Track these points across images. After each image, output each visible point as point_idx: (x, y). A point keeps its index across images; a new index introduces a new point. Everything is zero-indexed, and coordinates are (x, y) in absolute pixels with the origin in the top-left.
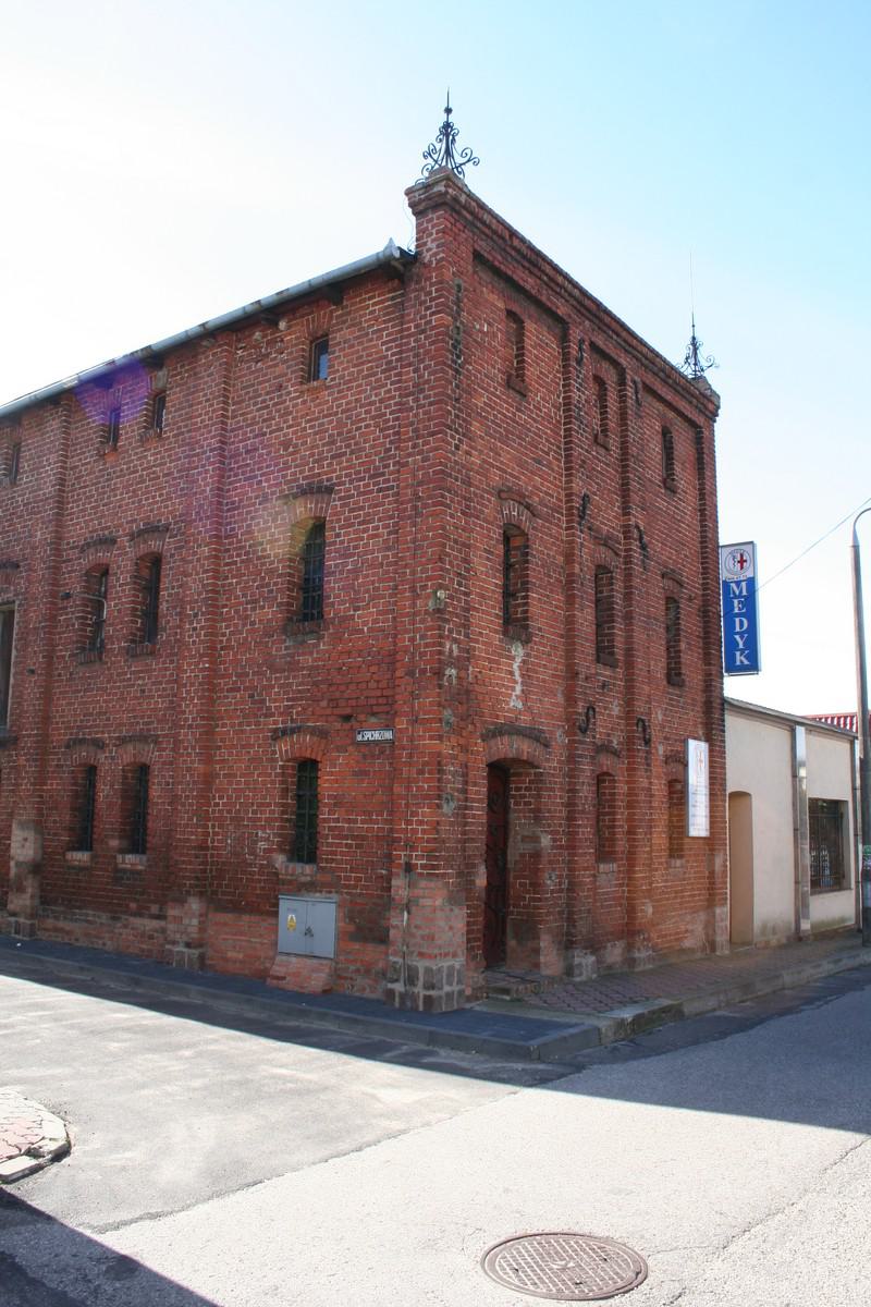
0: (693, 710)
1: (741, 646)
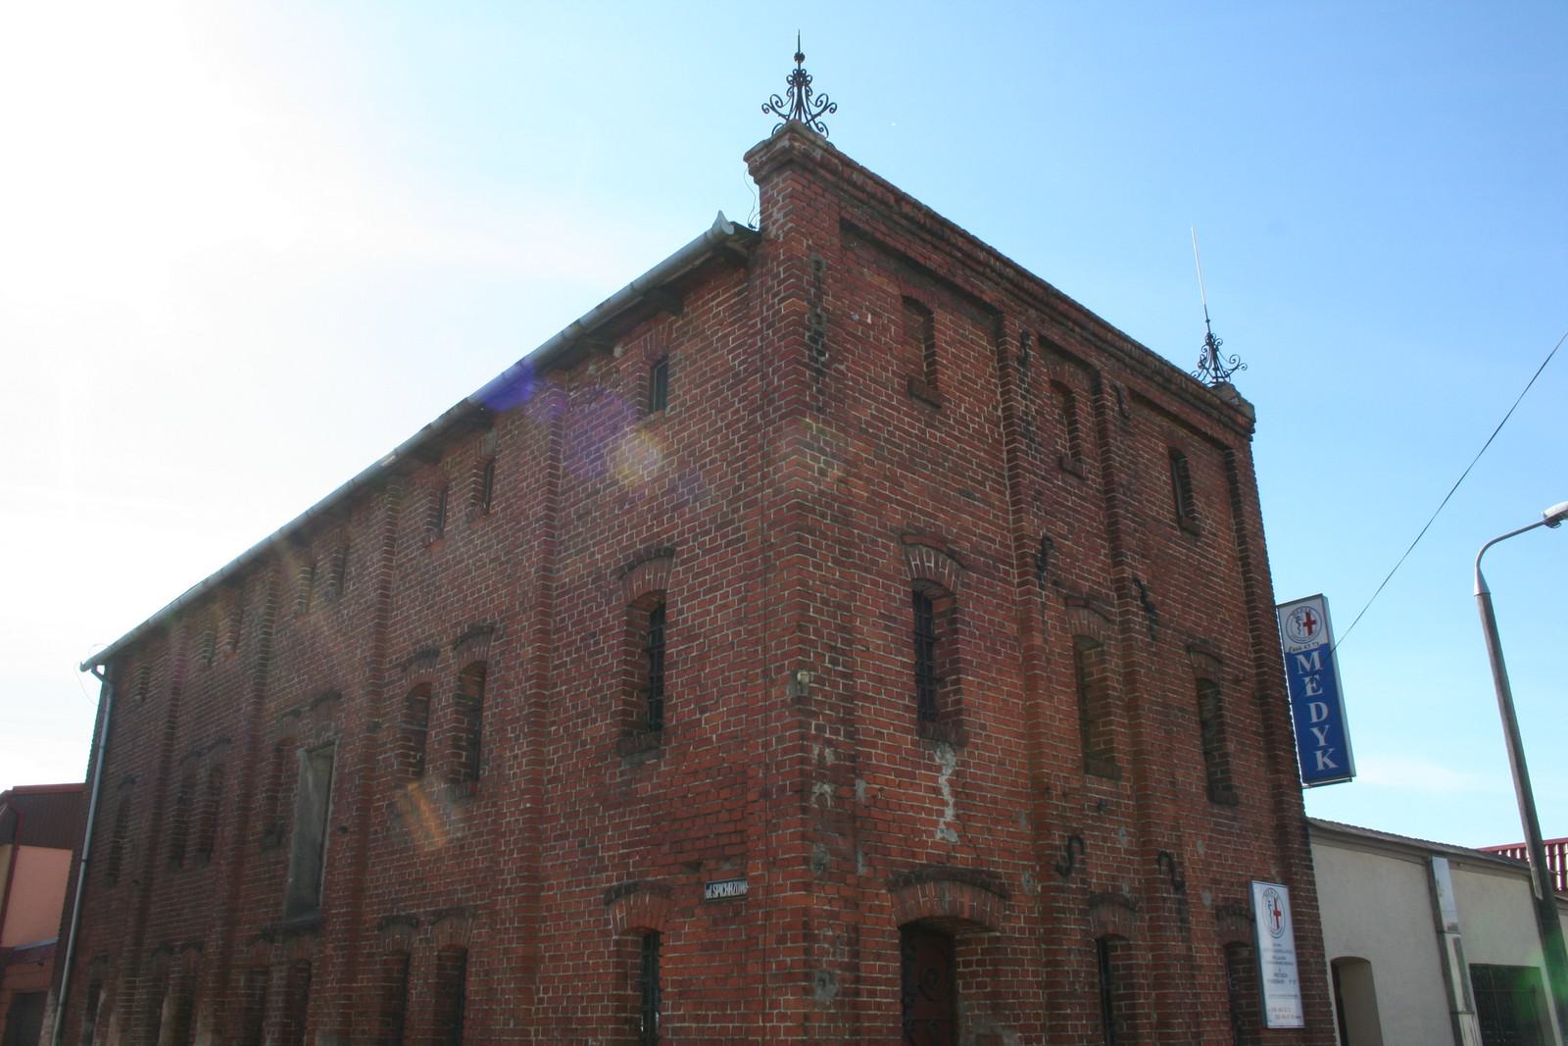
0: (1257, 839)
1: (1322, 743)
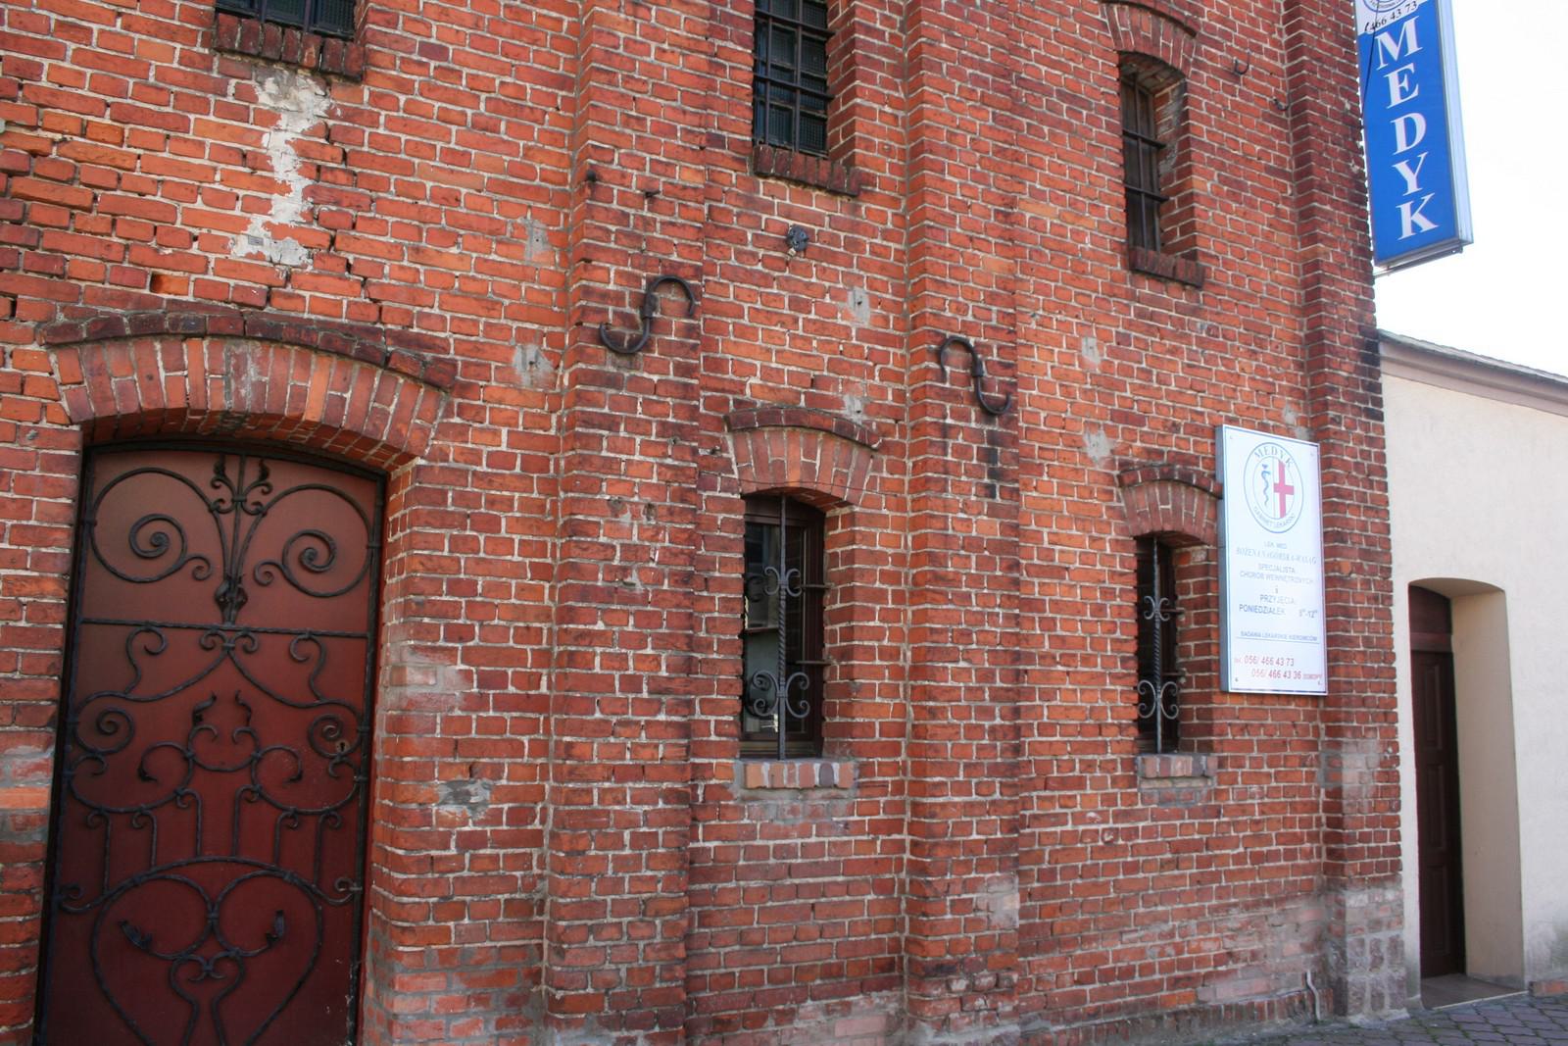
1: (1413, 187)
